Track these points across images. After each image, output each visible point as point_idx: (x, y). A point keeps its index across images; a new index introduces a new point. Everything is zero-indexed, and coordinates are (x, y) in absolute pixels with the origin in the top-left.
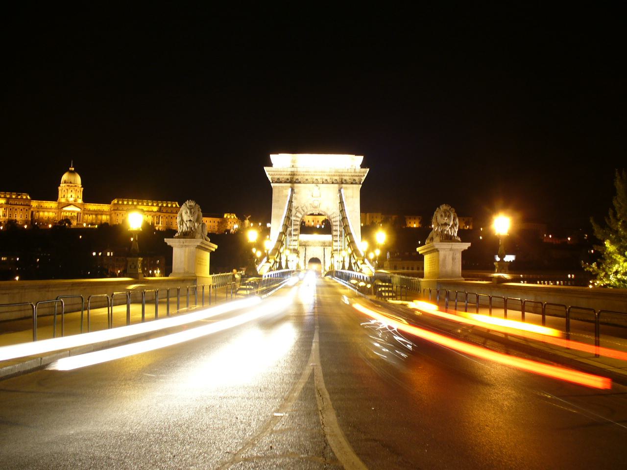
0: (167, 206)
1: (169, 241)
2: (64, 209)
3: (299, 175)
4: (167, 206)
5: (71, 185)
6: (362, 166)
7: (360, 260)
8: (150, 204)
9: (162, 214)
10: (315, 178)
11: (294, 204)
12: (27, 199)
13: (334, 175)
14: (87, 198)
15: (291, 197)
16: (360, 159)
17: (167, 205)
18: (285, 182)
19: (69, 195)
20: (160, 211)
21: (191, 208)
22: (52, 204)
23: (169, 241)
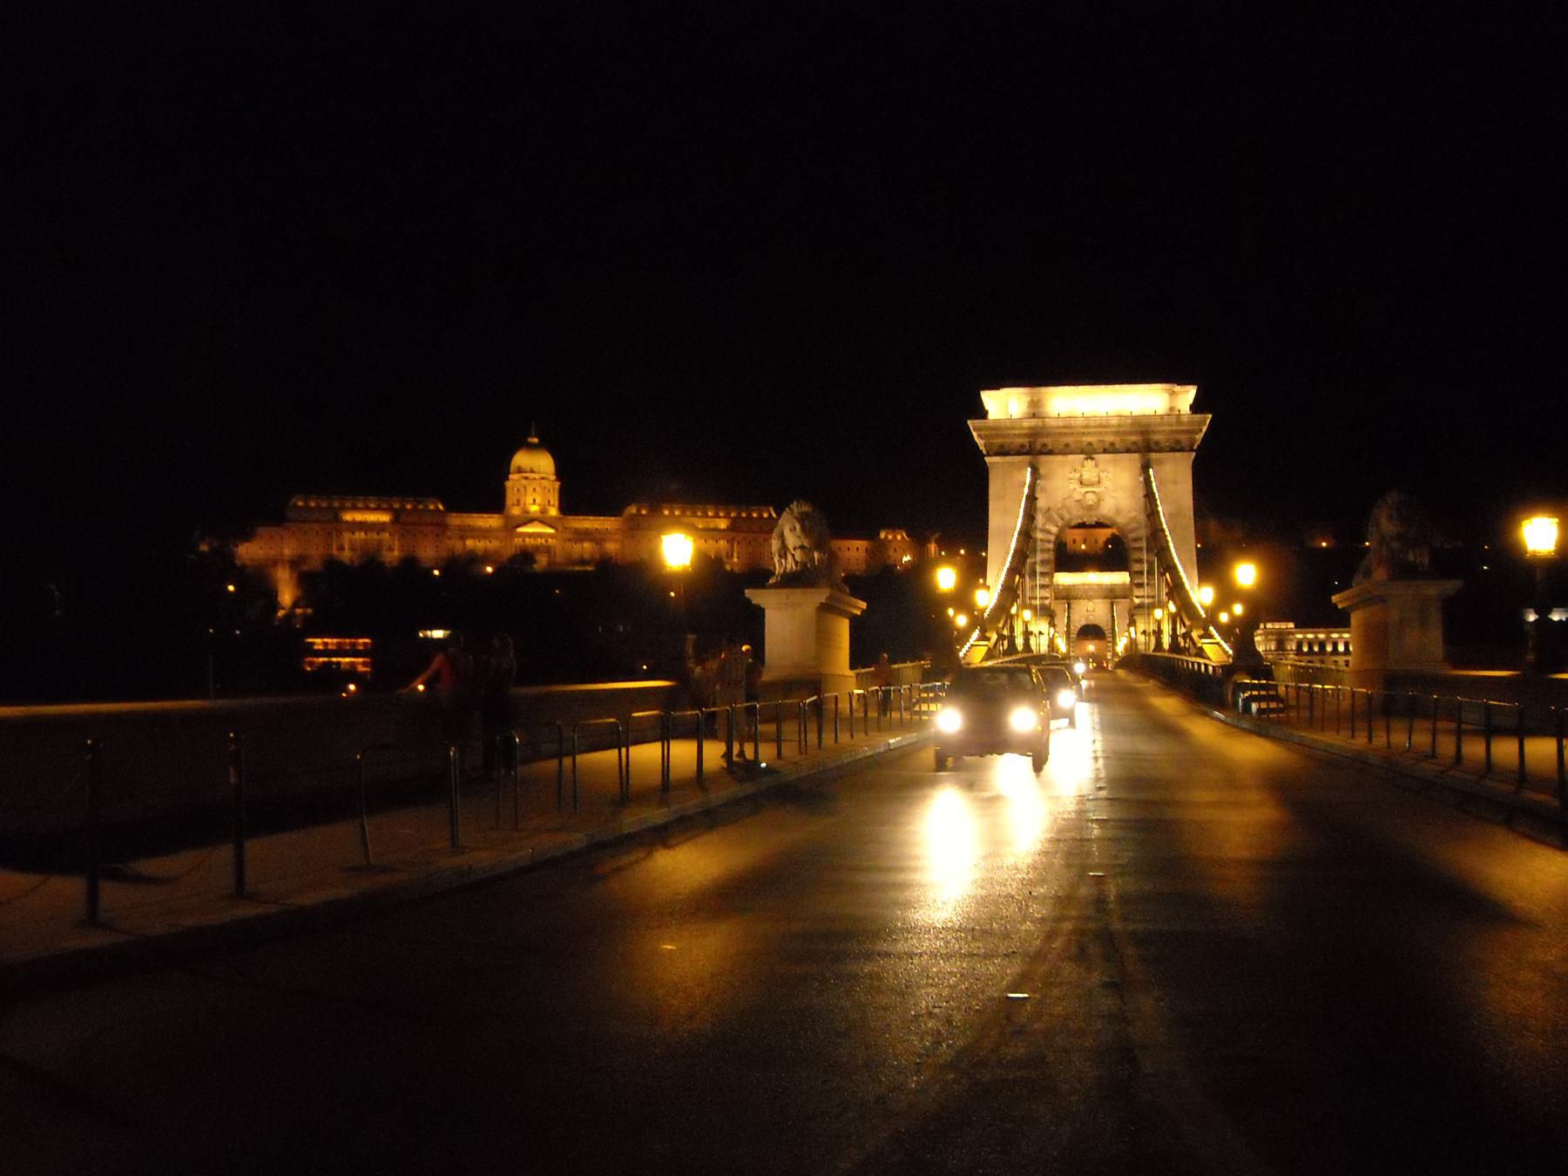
1: (756, 596)
2: (520, 530)
3: (1048, 435)
6: (1196, 407)
7: (1197, 628)
9: (740, 537)
10: (1086, 439)
11: (1042, 503)
13: (1131, 433)
14: (570, 504)
15: (1033, 487)
16: (1188, 394)
17: (750, 515)
18: (1018, 453)
20: (731, 528)
21: (802, 518)
22: (492, 521)
23: (756, 596)
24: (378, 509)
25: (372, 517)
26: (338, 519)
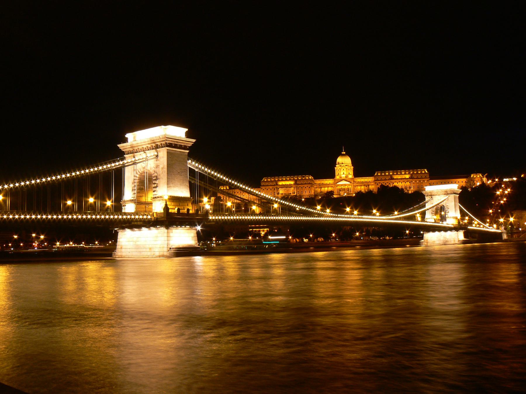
0: (417, 173)
4: (417, 173)
5: (342, 165)
8: (403, 173)
12: (309, 179)
14: (357, 174)
18: (131, 153)
19: (342, 173)
20: (411, 178)
22: (330, 181)
24: (290, 180)
25: (288, 183)
26: (277, 185)
